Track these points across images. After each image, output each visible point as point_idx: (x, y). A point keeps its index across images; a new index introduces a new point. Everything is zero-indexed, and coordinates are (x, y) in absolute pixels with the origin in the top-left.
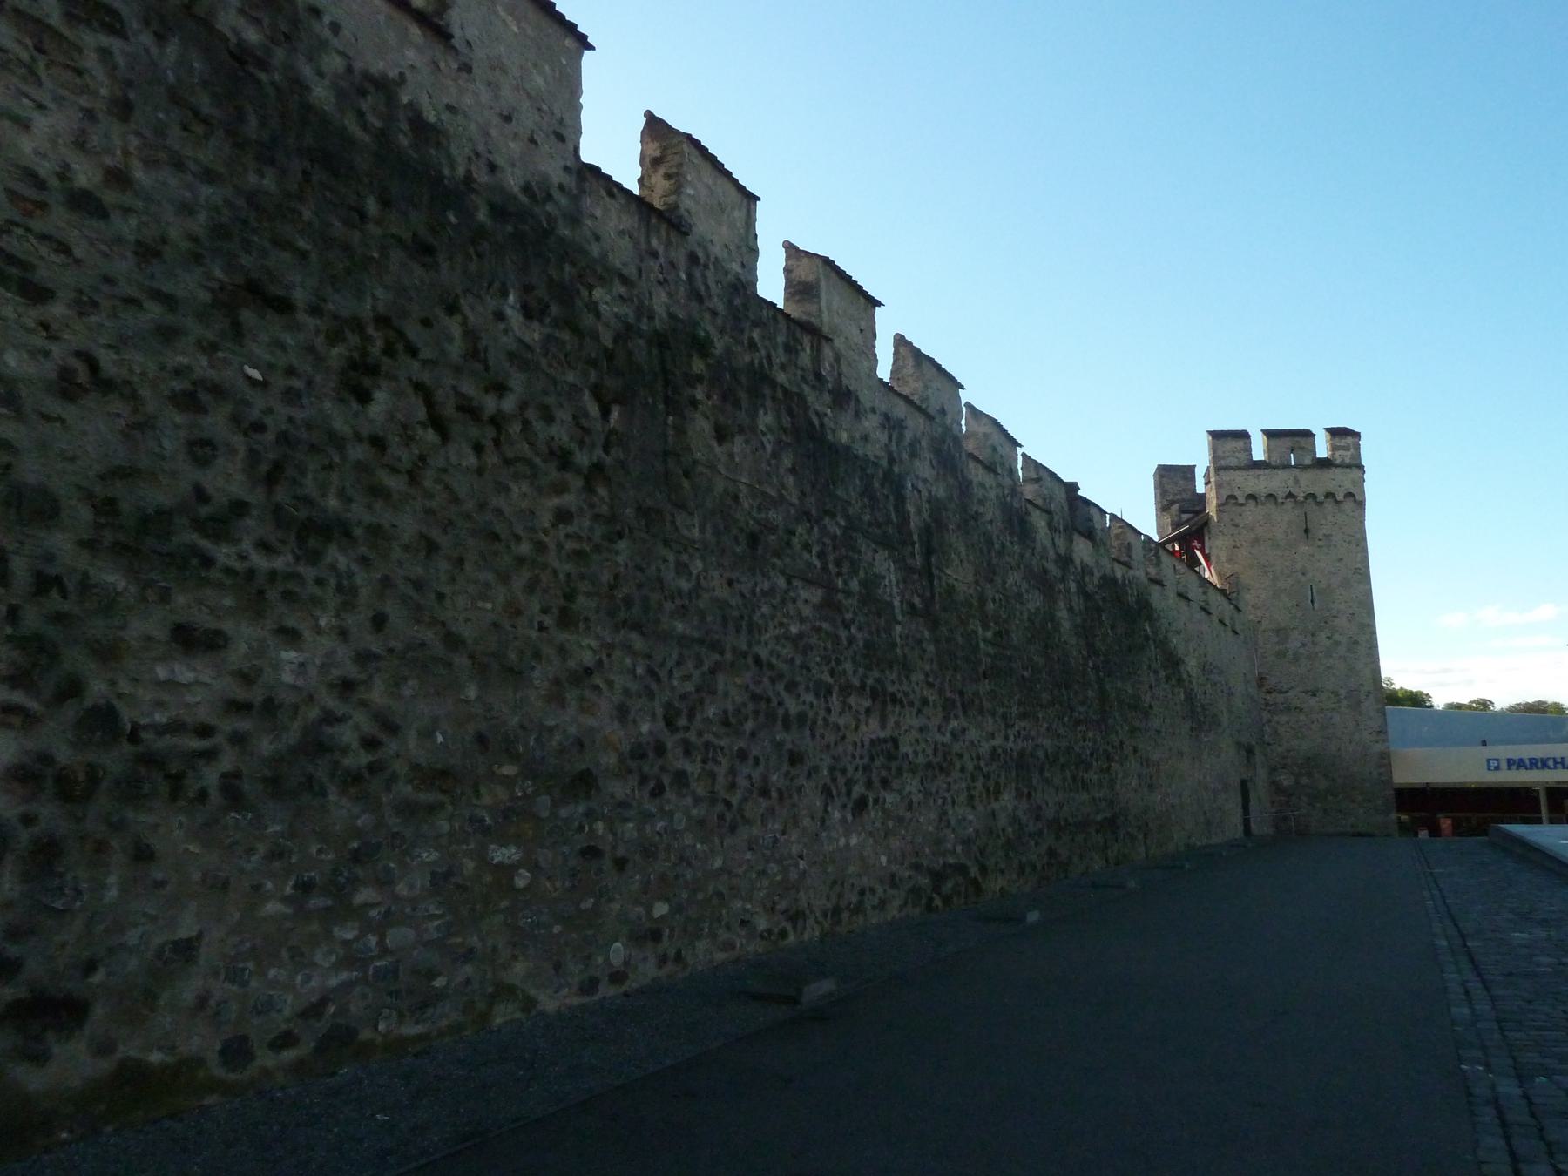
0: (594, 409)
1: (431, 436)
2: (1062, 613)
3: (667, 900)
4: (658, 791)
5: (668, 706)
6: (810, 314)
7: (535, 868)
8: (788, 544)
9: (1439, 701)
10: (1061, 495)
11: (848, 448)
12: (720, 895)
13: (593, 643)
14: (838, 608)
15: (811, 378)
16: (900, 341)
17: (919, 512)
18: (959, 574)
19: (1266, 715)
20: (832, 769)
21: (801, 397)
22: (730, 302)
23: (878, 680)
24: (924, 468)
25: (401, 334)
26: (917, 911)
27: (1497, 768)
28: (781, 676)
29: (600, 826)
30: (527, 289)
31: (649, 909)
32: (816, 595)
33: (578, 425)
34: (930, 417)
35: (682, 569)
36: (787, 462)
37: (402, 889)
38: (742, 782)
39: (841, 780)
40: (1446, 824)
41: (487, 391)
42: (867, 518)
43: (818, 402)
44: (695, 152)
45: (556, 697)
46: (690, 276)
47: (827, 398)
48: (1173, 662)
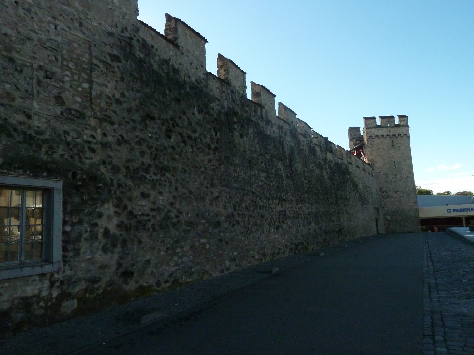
0: (214, 134)
1: (183, 145)
2: (325, 174)
3: (237, 251)
4: (233, 225)
5: (234, 205)
6: (259, 101)
7: (209, 244)
8: (258, 162)
9: (435, 193)
10: (323, 141)
11: (270, 135)
12: (248, 250)
13: (218, 191)
14: (270, 178)
15: (260, 118)
16: (280, 104)
17: (288, 150)
18: (298, 166)
19: (382, 199)
20: (271, 219)
21: (259, 124)
22: (241, 102)
23: (280, 195)
24: (288, 138)
25: (176, 122)
26: (292, 254)
27: (450, 212)
28: (258, 196)
29: (222, 234)
30: (199, 106)
31: (233, 253)
32: (264, 175)
33: (211, 138)
34: (289, 124)
35: (235, 171)
36: (256, 141)
37: (185, 249)
38: (251, 223)
39: (273, 221)
40: (436, 229)
41: (193, 132)
42: (275, 153)
43: (262, 124)
44: (231, 64)
45: (211, 204)
46: (232, 96)
47: (264, 123)
48: (355, 186)
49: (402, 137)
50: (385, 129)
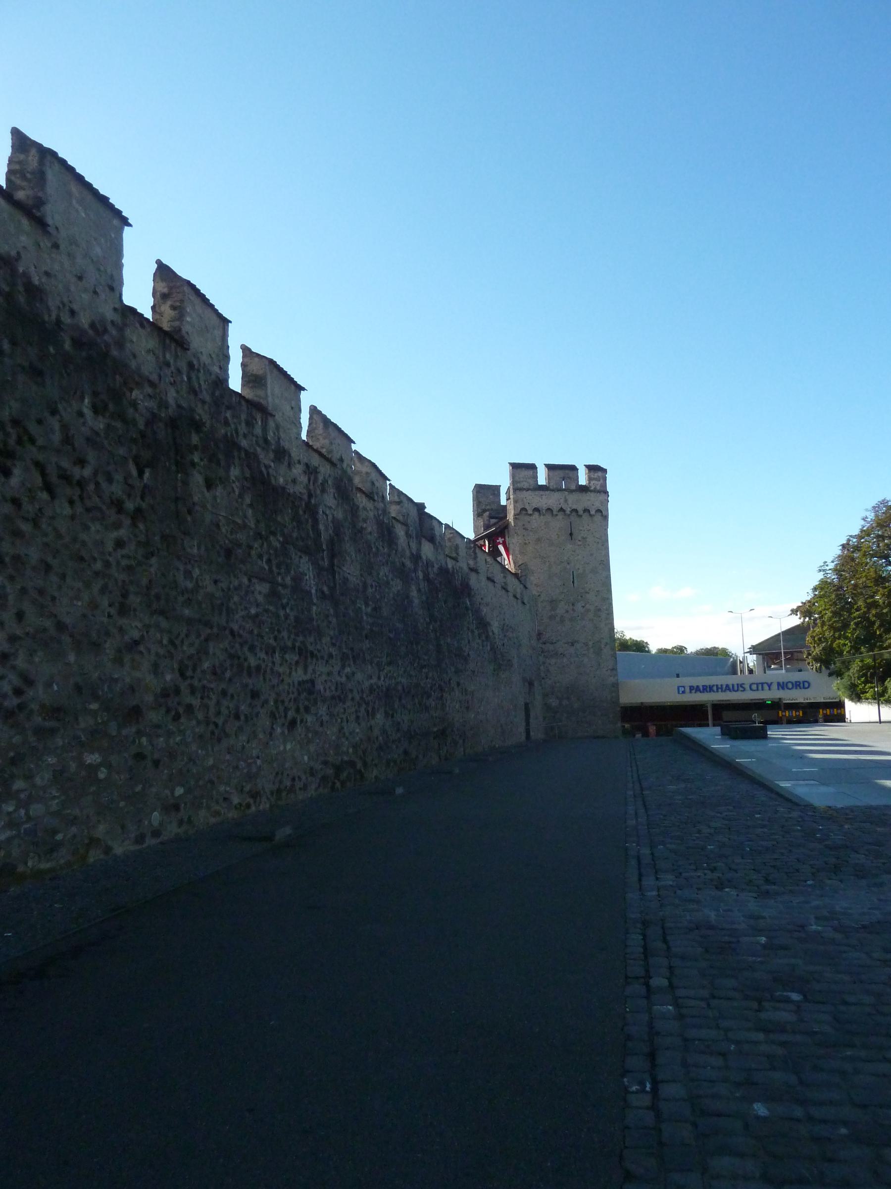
0: (135, 473)
1: (45, 496)
2: (414, 593)
3: (183, 786)
4: (177, 718)
5: (181, 662)
7: (109, 766)
8: (249, 554)
9: (653, 648)
10: (414, 513)
11: (284, 489)
12: (211, 782)
13: (139, 625)
15: (261, 442)
16: (314, 410)
17: (327, 529)
18: (351, 571)
19: (541, 659)
20: (276, 702)
21: (256, 455)
22: (213, 394)
24: (330, 499)
25: (26, 431)
27: (683, 692)
28: (246, 642)
29: (144, 740)
30: (95, 394)
31: (172, 792)
33: (126, 483)
34: (333, 464)
35: (188, 574)
36: (248, 500)
37: (38, 781)
38: (225, 711)
39: (281, 708)
40: (652, 729)
41: (75, 464)
42: (295, 535)
43: (266, 458)
45: (118, 661)
46: (189, 378)
47: (271, 455)
48: (483, 624)
49: (591, 515)
50: (557, 495)
